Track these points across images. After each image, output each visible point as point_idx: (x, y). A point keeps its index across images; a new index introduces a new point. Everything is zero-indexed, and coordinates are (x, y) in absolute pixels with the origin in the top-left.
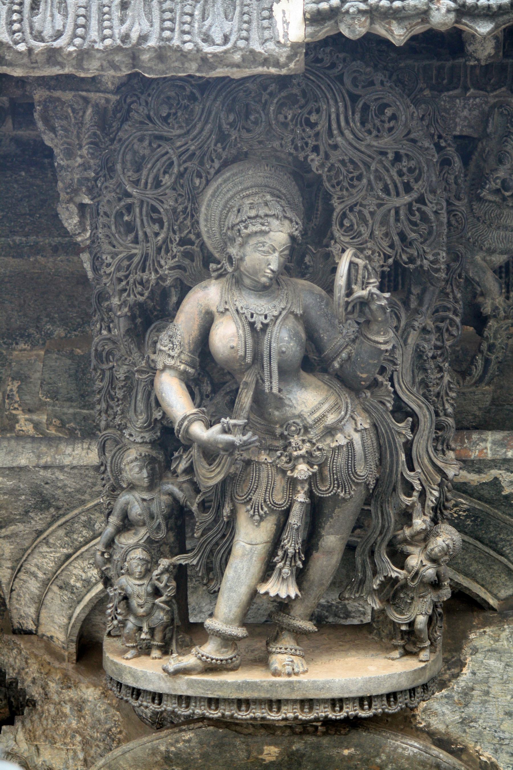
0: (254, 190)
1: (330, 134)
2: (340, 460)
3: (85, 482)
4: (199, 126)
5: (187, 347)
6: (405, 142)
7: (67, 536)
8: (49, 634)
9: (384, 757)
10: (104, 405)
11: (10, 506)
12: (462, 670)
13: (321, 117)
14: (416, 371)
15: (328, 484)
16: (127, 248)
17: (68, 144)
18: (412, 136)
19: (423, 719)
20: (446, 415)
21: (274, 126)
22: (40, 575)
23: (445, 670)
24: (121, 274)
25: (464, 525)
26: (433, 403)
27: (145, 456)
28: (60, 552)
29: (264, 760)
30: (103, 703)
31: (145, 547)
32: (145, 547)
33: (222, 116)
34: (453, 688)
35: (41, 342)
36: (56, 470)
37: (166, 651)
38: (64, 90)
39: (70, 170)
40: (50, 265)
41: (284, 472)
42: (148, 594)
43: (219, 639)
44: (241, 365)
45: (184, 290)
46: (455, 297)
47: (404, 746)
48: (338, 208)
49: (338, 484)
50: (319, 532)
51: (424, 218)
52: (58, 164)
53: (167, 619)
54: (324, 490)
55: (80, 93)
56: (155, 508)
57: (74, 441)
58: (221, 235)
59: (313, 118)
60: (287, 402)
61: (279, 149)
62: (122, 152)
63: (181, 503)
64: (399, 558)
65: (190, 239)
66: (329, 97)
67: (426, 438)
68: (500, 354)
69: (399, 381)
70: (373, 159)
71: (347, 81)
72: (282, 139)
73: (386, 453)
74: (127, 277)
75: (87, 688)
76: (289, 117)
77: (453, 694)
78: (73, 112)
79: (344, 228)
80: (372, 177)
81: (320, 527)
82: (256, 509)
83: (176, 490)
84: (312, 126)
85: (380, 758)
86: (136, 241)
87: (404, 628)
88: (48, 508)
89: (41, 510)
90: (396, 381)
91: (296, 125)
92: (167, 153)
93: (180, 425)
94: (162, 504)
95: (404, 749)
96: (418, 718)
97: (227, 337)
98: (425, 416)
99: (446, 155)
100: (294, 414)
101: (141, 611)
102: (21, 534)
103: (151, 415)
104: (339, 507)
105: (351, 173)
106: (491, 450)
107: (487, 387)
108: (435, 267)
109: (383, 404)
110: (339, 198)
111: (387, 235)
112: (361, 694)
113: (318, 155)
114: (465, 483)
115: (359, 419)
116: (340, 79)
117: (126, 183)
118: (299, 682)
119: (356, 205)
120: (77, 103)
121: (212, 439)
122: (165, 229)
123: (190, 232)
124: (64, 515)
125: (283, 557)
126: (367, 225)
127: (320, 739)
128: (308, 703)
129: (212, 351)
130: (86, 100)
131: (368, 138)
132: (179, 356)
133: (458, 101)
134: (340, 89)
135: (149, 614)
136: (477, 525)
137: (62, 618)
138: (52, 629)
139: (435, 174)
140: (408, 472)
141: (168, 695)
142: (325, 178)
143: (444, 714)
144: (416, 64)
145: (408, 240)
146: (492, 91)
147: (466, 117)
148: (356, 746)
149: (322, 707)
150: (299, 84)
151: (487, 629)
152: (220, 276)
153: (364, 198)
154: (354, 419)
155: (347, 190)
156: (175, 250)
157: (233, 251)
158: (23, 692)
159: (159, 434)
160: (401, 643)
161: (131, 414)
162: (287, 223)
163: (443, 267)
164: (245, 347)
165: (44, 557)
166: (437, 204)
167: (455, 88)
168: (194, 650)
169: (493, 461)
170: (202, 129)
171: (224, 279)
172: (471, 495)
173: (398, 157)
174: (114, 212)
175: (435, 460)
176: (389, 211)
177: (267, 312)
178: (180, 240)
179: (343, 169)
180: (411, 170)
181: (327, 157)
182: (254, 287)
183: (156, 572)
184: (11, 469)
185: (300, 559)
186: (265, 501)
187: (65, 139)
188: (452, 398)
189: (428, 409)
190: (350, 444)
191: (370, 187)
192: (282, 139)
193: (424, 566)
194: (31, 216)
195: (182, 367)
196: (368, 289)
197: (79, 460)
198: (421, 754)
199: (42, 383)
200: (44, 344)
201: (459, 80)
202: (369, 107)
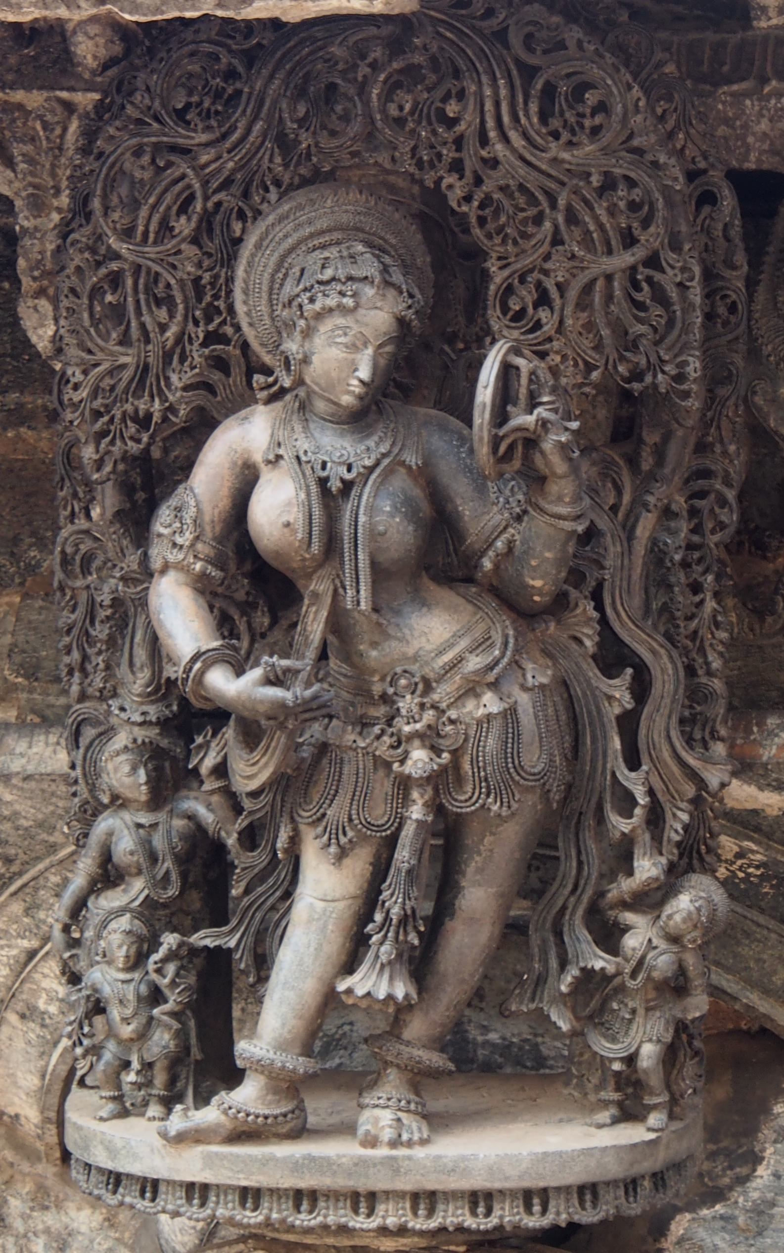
0: (336, 235)
1: (484, 141)
2: (491, 743)
3: (51, 808)
4: (241, 125)
5: (208, 528)
6: (624, 154)
7: (27, 915)
8: (11, 1111)
10: (76, 655)
12: (755, 1170)
13: (465, 108)
14: (653, 590)
15: (469, 788)
16: (112, 354)
17: (36, 187)
20: (710, 673)
21: (379, 124)
23: (724, 1170)
24: (98, 404)
26: (686, 652)
27: (143, 742)
28: (17, 947)
30: (107, 1237)
31: (140, 913)
32: (140, 913)
33: (284, 106)
34: (736, 1202)
35: (17, 581)
37: (169, 1102)
38: (28, 88)
39: (38, 235)
40: (44, 445)
41: (388, 765)
42: (139, 998)
43: (262, 1077)
44: (304, 560)
46: (725, 453)
48: (498, 277)
49: (488, 787)
50: (457, 882)
52: (22, 227)
53: (176, 1046)
54: (463, 802)
55: (59, 93)
56: (159, 841)
57: (32, 732)
58: (273, 319)
59: (452, 109)
60: (391, 630)
61: (388, 165)
62: (102, 176)
63: (210, 832)
64: (609, 936)
65: (225, 335)
66: (481, 69)
67: (667, 712)
69: (614, 602)
71: (515, 40)
72: (395, 148)
73: (584, 734)
74: (108, 408)
75: (79, 1209)
76: (408, 107)
77: (737, 1212)
78: (45, 129)
79: (511, 314)
80: (561, 219)
82: (333, 834)
83: (201, 811)
87: (617, 1066)
90: (607, 601)
91: (419, 123)
92: (183, 177)
93: (188, 670)
94: (174, 833)
97: (278, 509)
98: (663, 671)
99: (707, 184)
100: (404, 654)
101: (127, 1031)
103: (161, 672)
104: (493, 834)
105: (523, 210)
108: (682, 387)
109: (579, 642)
110: (499, 258)
111: (589, 326)
112: (526, 1184)
114: (755, 812)
116: (501, 36)
117: (109, 233)
118: (409, 1158)
119: (531, 271)
120: (53, 111)
121: (244, 697)
122: (179, 317)
123: (224, 322)
124: (20, 874)
125: (383, 925)
126: (552, 309)
128: (426, 1199)
129: (252, 533)
130: (69, 107)
131: (553, 145)
132: (192, 545)
133: (748, 102)
134: (501, 55)
137: (29, 1077)
138: (16, 1100)
139: (687, 220)
140: (626, 772)
141: (168, 1182)
142: (473, 220)
144: (675, 39)
145: (630, 337)
149: (451, 1207)
150: (425, 47)
152: (271, 400)
153: (547, 257)
154: (520, 667)
155: (515, 243)
156: (195, 354)
157: (292, 346)
159: (175, 708)
160: (615, 1096)
161: (123, 671)
162: (391, 293)
163: (694, 387)
164: (310, 523)
166: (683, 269)
167: (743, 79)
168: (215, 1100)
170: (248, 131)
171: (278, 405)
174: (88, 287)
175: (684, 754)
176: (593, 281)
177: (351, 460)
178: (205, 338)
179: (506, 203)
180: (634, 206)
182: (333, 415)
183: (155, 957)
185: (415, 928)
186: (350, 820)
187: (29, 179)
188: (721, 642)
189: (671, 657)
192: (395, 148)
193: (655, 948)
194: (12, 357)
196: (536, 412)
197: (39, 764)
199: (11, 650)
200: (22, 584)
201: (752, 64)
202: (555, 88)
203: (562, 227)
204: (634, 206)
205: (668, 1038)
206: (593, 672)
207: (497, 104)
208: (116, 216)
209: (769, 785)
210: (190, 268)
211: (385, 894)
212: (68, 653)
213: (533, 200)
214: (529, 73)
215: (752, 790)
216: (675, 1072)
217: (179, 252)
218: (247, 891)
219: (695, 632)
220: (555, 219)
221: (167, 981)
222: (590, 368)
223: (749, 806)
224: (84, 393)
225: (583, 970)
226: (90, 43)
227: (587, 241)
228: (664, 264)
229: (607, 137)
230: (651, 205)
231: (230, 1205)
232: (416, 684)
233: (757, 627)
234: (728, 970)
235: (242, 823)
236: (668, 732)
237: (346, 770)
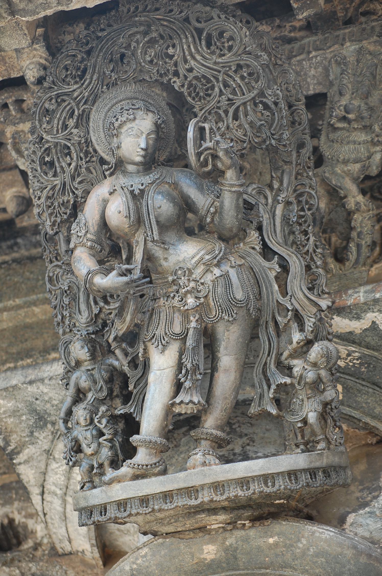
1: (186, 61)
2: (220, 290)
8: (80, 549)
9: (305, 542)
10: (60, 317)
11: (18, 429)
18: (247, 49)
19: (351, 531)
20: (317, 267)
22: (59, 492)
23: (367, 495)
25: (360, 372)
29: (206, 559)
36: (39, 384)
38: (24, 122)
45: (88, 192)
47: (321, 530)
51: (266, 107)
56: (97, 376)
59: (171, 51)
68: (368, 239)
69: (268, 236)
70: (219, 72)
73: (262, 287)
74: (52, 203)
76: (153, 54)
77: (375, 510)
80: (221, 86)
81: (217, 351)
85: (302, 543)
86: (55, 175)
87: (299, 425)
88: (45, 425)
89: (42, 428)
92: (69, 104)
95: (321, 533)
96: (347, 530)
101: (89, 451)
102: (35, 456)
103: (92, 312)
106: (363, 297)
107: (364, 268)
109: (253, 248)
113: (179, 78)
114: (351, 333)
115: (232, 259)
116: (187, 20)
122: (75, 159)
127: (247, 531)
133: (304, 63)
135: (96, 453)
136: (371, 371)
138: (81, 542)
140: (282, 298)
143: (368, 525)
146: (328, 49)
147: (314, 76)
148: (278, 534)
162: (150, 115)
165: (56, 473)
167: (301, 54)
169: (365, 303)
170: (91, 78)
172: (360, 345)
173: (239, 67)
181: (186, 77)
183: (97, 417)
184: (6, 389)
189: (297, 257)
190: (226, 276)
191: (221, 93)
193: (306, 369)
195: (89, 244)
198: (337, 537)
203: (222, 88)
204: (250, 74)
205: (320, 408)
206: (261, 260)
208: (44, 126)
209: (353, 317)
210: (76, 138)
211: (184, 360)
212: (56, 317)
213: (209, 81)
214: (199, 32)
215: (347, 321)
216: (328, 430)
217: (72, 133)
218: (135, 387)
219: (308, 251)
220: (219, 86)
221: (103, 425)
223: (348, 330)
224: (43, 200)
225: (278, 386)
226: (31, 72)
227: (234, 92)
228: (267, 95)
229: (235, 49)
230: (258, 73)
231: (137, 507)
232: (185, 272)
233: (343, 268)
234: (354, 408)
235: (129, 358)
236: (301, 287)
237: (162, 315)
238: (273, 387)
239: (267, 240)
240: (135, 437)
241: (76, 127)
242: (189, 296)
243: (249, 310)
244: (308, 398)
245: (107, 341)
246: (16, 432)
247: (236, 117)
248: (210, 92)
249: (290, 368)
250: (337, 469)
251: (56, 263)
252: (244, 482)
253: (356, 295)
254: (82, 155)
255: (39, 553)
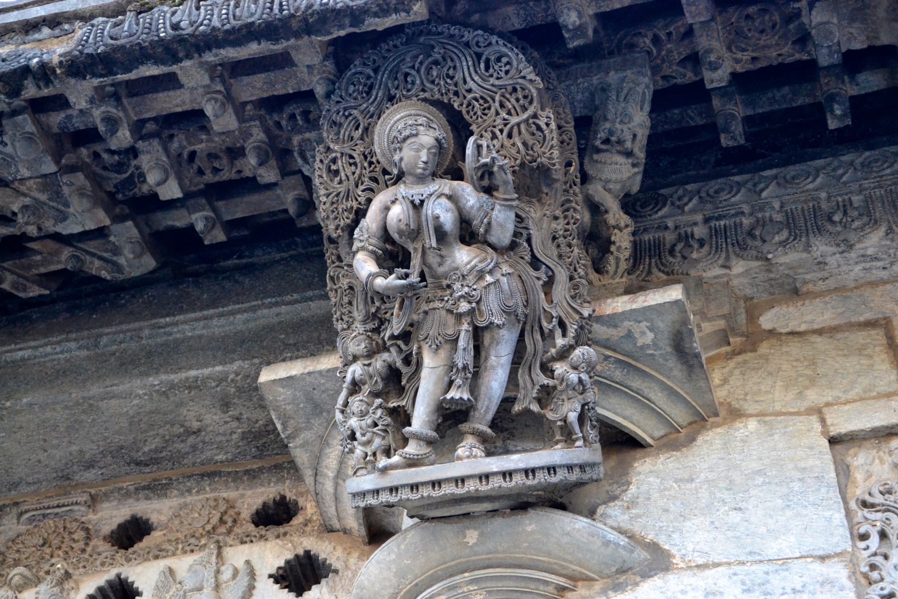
1: (465, 82)
38: (310, 132)
45: (369, 201)
51: (539, 128)
74: (336, 208)
84: (452, 78)
86: (340, 182)
87: (559, 423)
142: (464, 112)
151: (647, 459)
157: (396, 158)
158: (330, 565)
169: (623, 313)
173: (515, 90)
191: (497, 114)
195: (371, 248)
207: (469, 69)
213: (486, 101)
215: (605, 328)
218: (407, 382)
222: (516, 159)
223: (605, 337)
224: (328, 205)
227: (509, 113)
235: (403, 355)
238: (537, 387)
239: (535, 251)
240: (407, 429)
241: (362, 139)
242: (462, 300)
243: (517, 316)
244: (569, 399)
245: (383, 338)
246: (294, 418)
247: (510, 136)
248: (486, 111)
249: (553, 371)
250: (593, 465)
251: (337, 264)
252: (507, 474)
253: (615, 305)
254: (366, 164)
255: (308, 529)
